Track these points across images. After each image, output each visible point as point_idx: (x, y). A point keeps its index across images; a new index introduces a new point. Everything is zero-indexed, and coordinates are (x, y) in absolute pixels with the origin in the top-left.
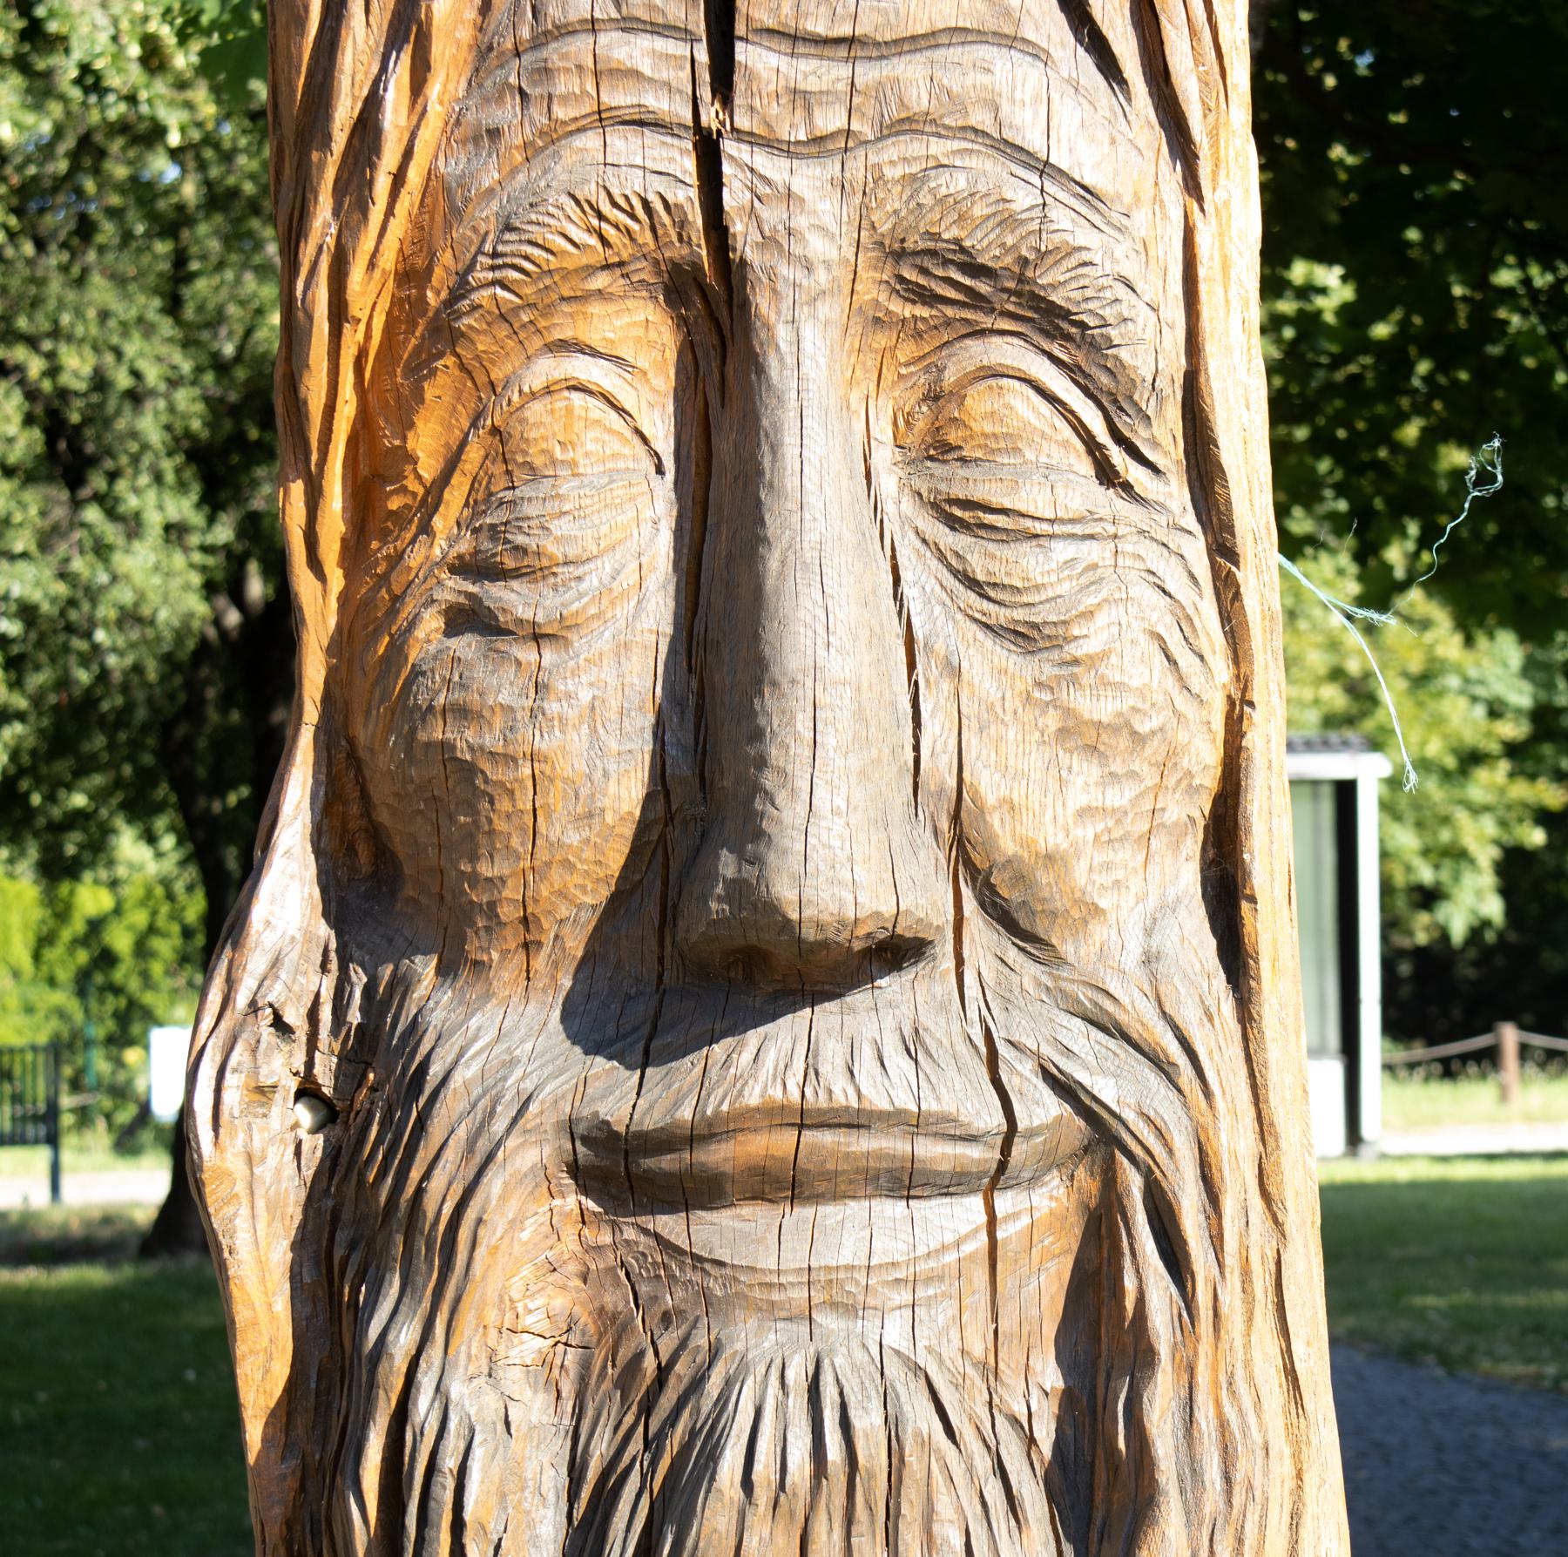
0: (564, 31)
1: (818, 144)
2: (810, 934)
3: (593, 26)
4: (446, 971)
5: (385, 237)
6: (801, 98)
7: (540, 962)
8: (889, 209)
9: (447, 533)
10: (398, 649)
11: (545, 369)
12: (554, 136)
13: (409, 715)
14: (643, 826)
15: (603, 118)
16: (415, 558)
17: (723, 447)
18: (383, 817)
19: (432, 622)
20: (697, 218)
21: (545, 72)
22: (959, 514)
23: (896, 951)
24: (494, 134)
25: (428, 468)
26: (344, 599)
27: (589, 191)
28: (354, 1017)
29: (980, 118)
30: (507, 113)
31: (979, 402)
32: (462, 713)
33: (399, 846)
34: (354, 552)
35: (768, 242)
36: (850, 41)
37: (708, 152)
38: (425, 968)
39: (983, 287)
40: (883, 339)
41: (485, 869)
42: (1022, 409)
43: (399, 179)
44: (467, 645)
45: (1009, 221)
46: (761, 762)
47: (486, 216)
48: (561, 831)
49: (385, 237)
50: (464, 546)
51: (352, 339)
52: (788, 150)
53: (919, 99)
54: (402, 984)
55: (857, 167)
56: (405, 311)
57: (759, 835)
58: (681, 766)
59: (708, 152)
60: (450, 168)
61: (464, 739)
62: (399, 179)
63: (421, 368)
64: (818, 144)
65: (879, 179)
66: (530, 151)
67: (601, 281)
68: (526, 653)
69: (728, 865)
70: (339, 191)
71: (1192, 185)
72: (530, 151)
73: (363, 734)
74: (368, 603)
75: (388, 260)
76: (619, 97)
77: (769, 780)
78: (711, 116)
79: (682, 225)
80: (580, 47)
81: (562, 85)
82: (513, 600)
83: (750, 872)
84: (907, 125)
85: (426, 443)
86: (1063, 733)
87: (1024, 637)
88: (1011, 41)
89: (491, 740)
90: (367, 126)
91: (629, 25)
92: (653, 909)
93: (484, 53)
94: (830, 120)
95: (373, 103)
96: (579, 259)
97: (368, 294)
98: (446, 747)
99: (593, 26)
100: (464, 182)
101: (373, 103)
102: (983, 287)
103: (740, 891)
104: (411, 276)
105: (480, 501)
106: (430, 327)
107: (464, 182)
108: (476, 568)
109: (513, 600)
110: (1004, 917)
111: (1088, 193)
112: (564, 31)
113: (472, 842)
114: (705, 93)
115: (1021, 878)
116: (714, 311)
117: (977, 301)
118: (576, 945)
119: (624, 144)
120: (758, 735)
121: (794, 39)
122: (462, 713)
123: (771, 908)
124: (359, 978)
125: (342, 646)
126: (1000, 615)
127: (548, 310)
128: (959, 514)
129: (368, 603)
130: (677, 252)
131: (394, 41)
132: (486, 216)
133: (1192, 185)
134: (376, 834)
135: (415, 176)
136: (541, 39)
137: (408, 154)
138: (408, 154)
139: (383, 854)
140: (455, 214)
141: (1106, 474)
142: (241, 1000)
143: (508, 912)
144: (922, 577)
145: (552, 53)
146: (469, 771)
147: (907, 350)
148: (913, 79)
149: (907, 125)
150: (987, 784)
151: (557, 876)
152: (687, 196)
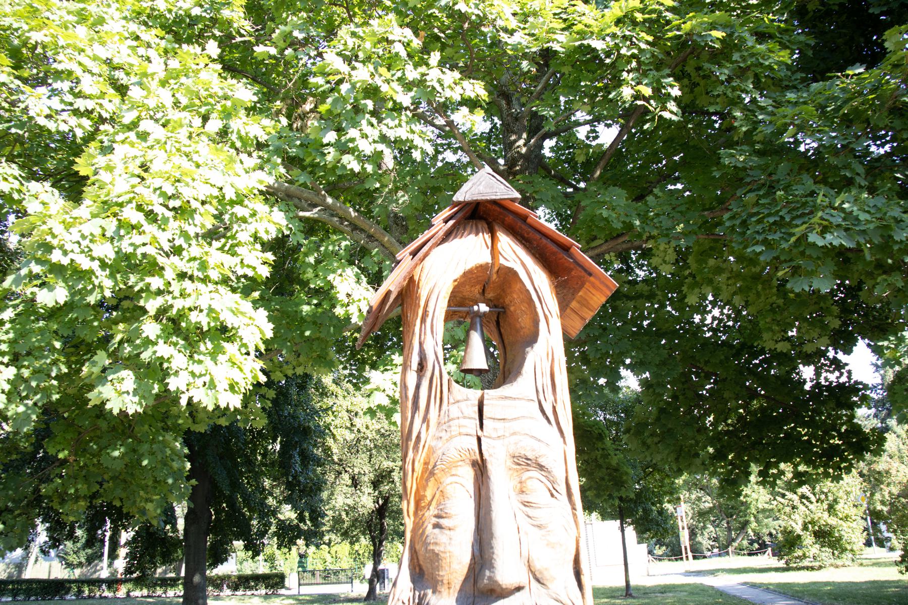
0: (453, 419)
2: (504, 587)
4: (434, 592)
5: (421, 457)
7: (451, 591)
8: (512, 449)
9: (433, 510)
10: (423, 532)
11: (450, 479)
12: (451, 438)
13: (426, 544)
14: (470, 565)
15: (460, 434)
16: (427, 514)
17: (483, 493)
18: (421, 563)
19: (430, 527)
20: (477, 452)
22: (526, 504)
23: (519, 589)
25: (429, 498)
26: (414, 522)
28: (417, 601)
30: (443, 434)
31: (529, 483)
32: (436, 544)
33: (424, 568)
34: (416, 513)
35: (491, 455)
37: (479, 440)
38: (429, 592)
39: (529, 462)
40: (511, 472)
41: (441, 573)
42: (535, 481)
44: (437, 531)
45: (533, 450)
46: (493, 553)
47: (439, 452)
48: (455, 566)
49: (421, 457)
50: (436, 512)
51: (415, 475)
52: (494, 439)
54: (425, 595)
56: (425, 470)
57: (493, 567)
58: (477, 553)
59: (479, 440)
60: (433, 443)
61: (437, 549)
63: (427, 480)
66: (447, 440)
67: (460, 463)
68: (447, 532)
69: (487, 573)
70: (414, 448)
72: (447, 440)
73: (417, 547)
74: (418, 523)
75: (422, 461)
77: (495, 556)
78: (480, 433)
80: (456, 422)
81: (453, 428)
82: (442, 522)
83: (492, 575)
84: (514, 434)
85: (429, 494)
86: (547, 545)
87: (539, 527)
89: (442, 549)
90: (418, 437)
91: (465, 417)
92: (472, 580)
95: (419, 433)
96: (456, 459)
97: (419, 467)
98: (433, 550)
101: (419, 433)
102: (529, 462)
103: (490, 578)
104: (426, 463)
105: (439, 504)
106: (429, 473)
108: (438, 516)
109: (442, 522)
110: (538, 581)
112: (453, 419)
113: (438, 568)
115: (541, 573)
116: (480, 468)
117: (528, 465)
118: (458, 587)
120: (492, 548)
122: (436, 544)
123: (496, 582)
124: (417, 593)
125: (414, 531)
126: (535, 523)
127: (451, 469)
128: (526, 504)
129: (418, 523)
130: (474, 458)
131: (424, 421)
132: (439, 452)
134: (420, 566)
136: (449, 421)
139: (421, 569)
140: (434, 452)
141: (552, 495)
142: (396, 599)
143: (445, 582)
144: (521, 517)
145: (451, 423)
146: (437, 555)
147: (516, 474)
149: (514, 434)
150: (533, 557)
151: (454, 574)
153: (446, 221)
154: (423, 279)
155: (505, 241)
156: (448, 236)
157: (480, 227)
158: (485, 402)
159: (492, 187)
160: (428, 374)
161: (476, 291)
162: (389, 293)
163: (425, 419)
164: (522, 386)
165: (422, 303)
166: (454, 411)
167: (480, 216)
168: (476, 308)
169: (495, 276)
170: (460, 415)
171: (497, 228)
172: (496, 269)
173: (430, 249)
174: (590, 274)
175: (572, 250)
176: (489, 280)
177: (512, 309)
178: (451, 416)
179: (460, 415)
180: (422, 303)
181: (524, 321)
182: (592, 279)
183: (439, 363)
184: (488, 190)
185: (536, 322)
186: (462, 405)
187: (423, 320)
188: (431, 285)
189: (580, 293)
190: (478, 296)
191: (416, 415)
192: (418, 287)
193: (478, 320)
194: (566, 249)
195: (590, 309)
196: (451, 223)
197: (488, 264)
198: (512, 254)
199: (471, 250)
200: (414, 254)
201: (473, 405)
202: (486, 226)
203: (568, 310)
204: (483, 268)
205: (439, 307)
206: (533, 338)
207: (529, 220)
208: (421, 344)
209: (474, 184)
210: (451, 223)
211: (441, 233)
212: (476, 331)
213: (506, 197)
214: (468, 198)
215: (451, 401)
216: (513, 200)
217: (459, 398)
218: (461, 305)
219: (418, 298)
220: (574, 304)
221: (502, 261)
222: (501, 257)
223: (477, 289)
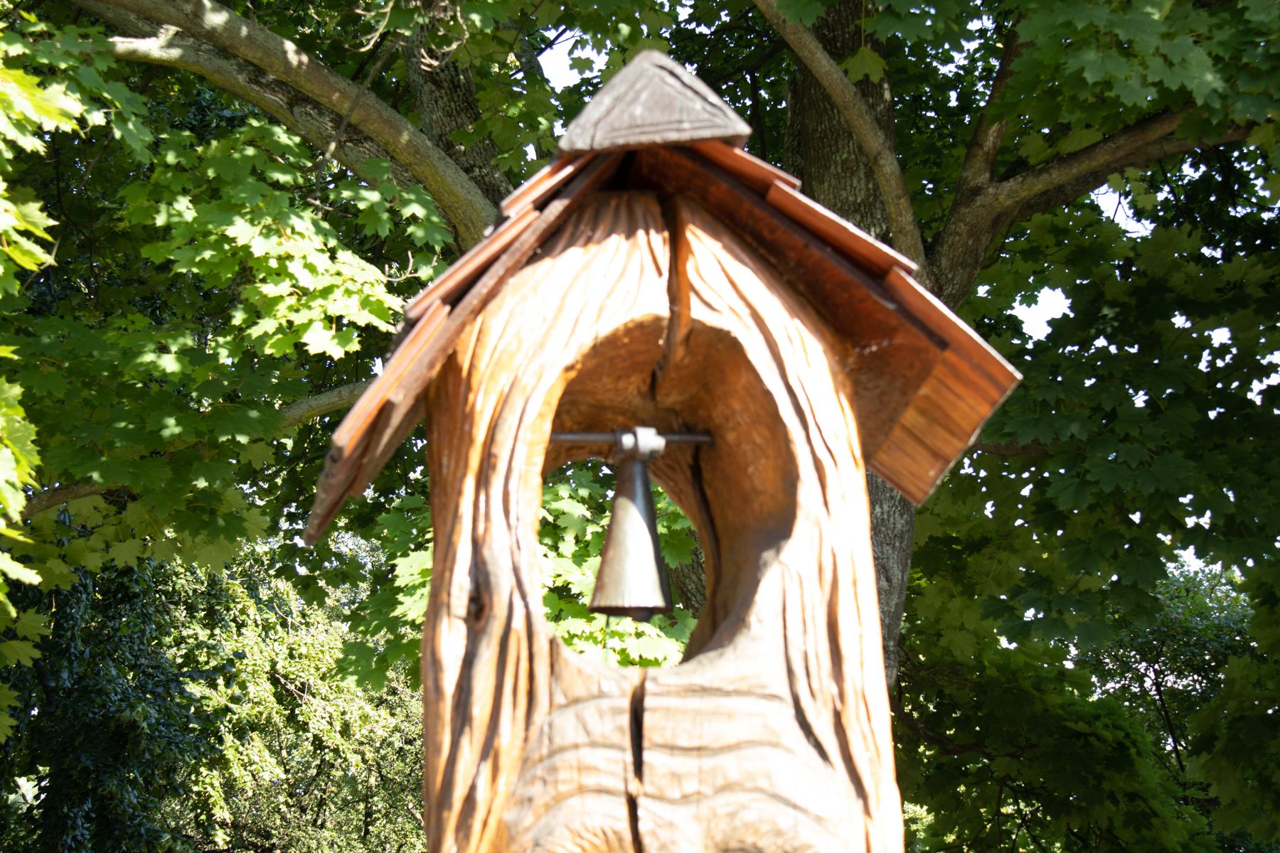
0: (562, 749)
1: (685, 798)
3: (576, 746)
6: (676, 777)
8: (721, 830)
12: (558, 799)
15: (582, 790)
20: (628, 837)
21: (553, 770)
24: (530, 800)
27: (576, 826)
29: (763, 783)
30: (536, 790)
36: (699, 749)
37: (632, 804)
43: (485, 824)
45: (779, 833)
47: (527, 839)
52: (672, 802)
53: (734, 776)
55: (705, 808)
59: (632, 804)
60: (509, 816)
62: (485, 824)
64: (685, 798)
65: (715, 815)
66: (548, 807)
71: (867, 811)
72: (548, 807)
76: (590, 780)
78: (634, 786)
79: (620, 840)
80: (570, 757)
81: (562, 775)
84: (727, 787)
88: (775, 745)
90: (470, 800)
91: (593, 745)
93: (525, 762)
94: (690, 787)
95: (473, 788)
99: (576, 746)
100: (516, 824)
101: (473, 788)
107: (516, 824)
111: (819, 819)
112: (562, 749)
114: (631, 774)
119: (592, 801)
121: (672, 748)
132: (527, 839)
133: (867, 811)
135: (492, 822)
136: (552, 754)
137: (489, 812)
138: (489, 812)
140: (512, 840)
148: (730, 766)
149: (727, 787)
152: (624, 826)
153: (541, 205)
154: (482, 365)
155: (708, 253)
156: (548, 242)
157: (639, 211)
158: (649, 702)
159: (668, 107)
160: (496, 628)
161: (632, 389)
162: (386, 409)
163: (489, 750)
164: (754, 653)
165: (480, 433)
166: (567, 728)
167: (634, 186)
168: (627, 440)
169: (680, 352)
170: (582, 738)
171: (685, 214)
172: (681, 333)
173: (501, 282)
174: (943, 344)
175: (891, 278)
176: (665, 357)
177: (731, 437)
178: (558, 741)
179: (582, 738)
180: (480, 433)
181: (761, 474)
182: (948, 355)
183: (524, 596)
184: (658, 116)
185: (790, 479)
186: (589, 711)
187: (483, 481)
188: (503, 383)
189: (924, 391)
190: (637, 401)
191: (465, 741)
192: (469, 388)
193: (637, 469)
194: (877, 272)
195: (953, 434)
196: (557, 207)
197: (658, 319)
198: (729, 289)
199: (613, 282)
200: (454, 299)
201: (616, 711)
202: (656, 209)
203: (897, 433)
204: (644, 331)
205: (525, 440)
206: (779, 527)
207: (772, 194)
208: (477, 545)
209: (618, 99)
210: (557, 207)
211: (529, 239)
212: (632, 498)
213: (707, 133)
214: (602, 140)
215: (560, 699)
216: (730, 141)
217: (579, 690)
218: (592, 423)
219: (469, 418)
220: (910, 417)
221: (698, 312)
222: (693, 297)
223: (633, 386)
